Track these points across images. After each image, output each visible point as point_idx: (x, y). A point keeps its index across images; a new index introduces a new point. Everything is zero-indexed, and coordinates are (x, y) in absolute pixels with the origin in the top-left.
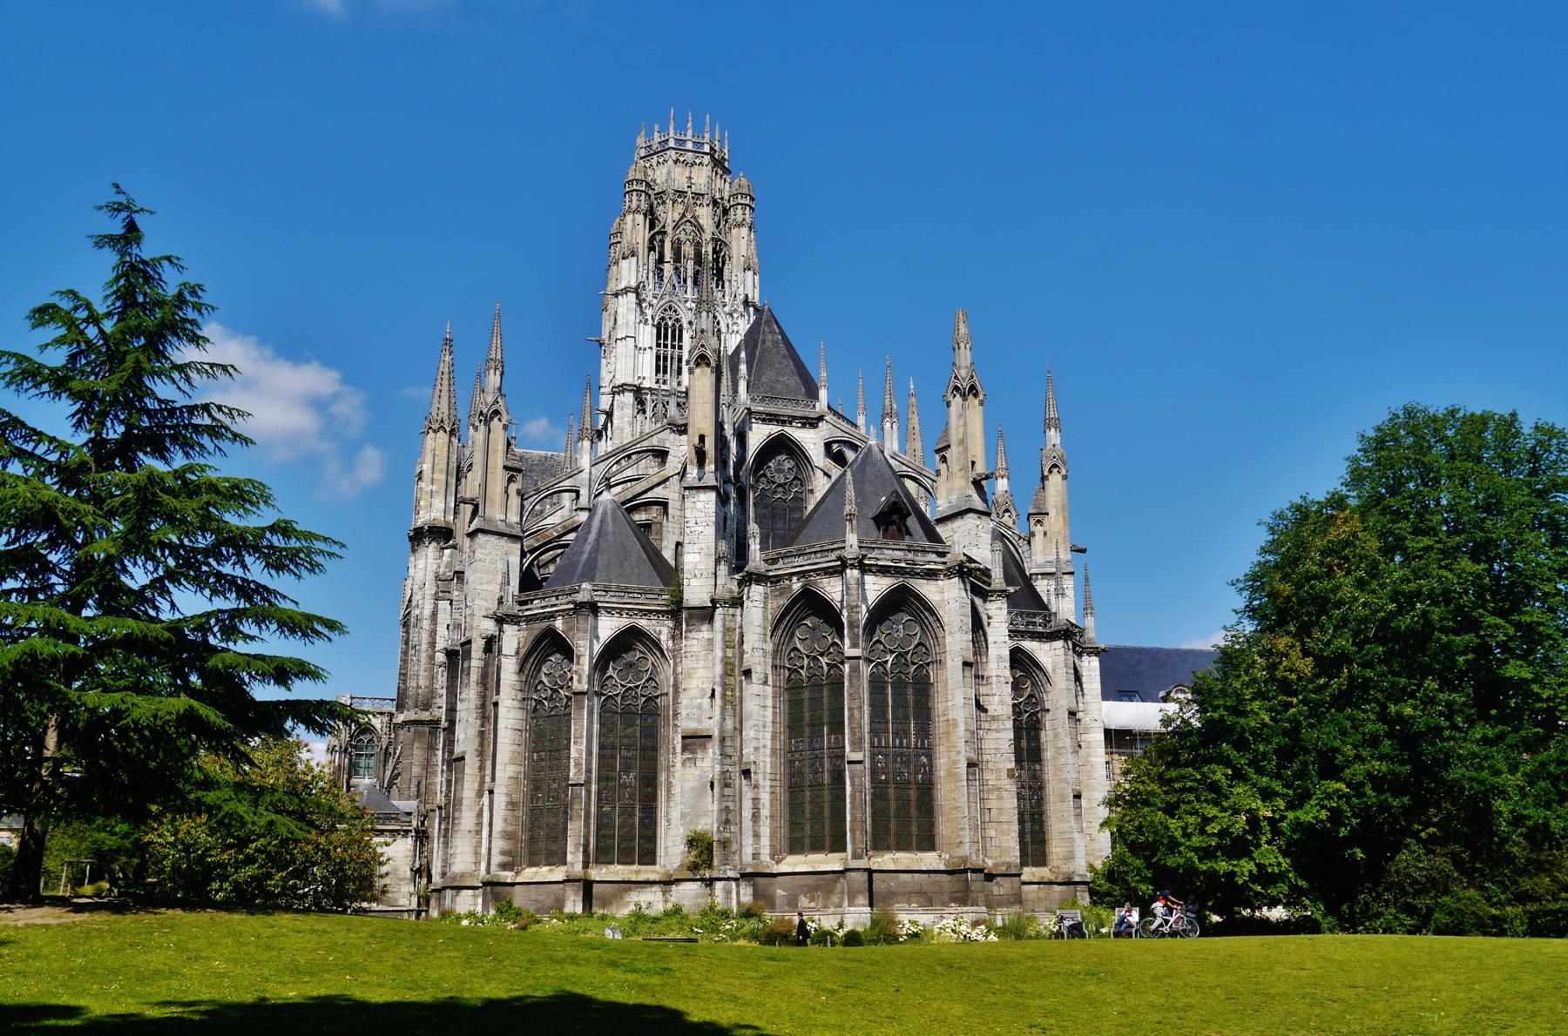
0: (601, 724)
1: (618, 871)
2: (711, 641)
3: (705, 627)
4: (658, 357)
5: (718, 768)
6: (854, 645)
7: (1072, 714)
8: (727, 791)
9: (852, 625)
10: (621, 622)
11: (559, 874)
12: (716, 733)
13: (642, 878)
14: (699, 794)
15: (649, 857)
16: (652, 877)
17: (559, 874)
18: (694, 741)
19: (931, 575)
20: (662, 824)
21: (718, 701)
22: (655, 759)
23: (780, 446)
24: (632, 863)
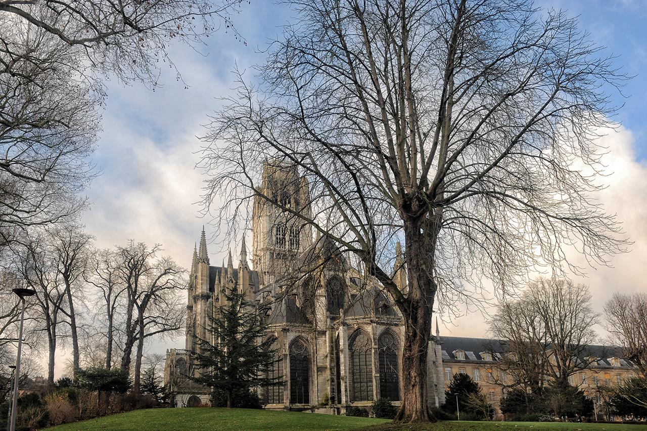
0: (291, 363)
1: (299, 405)
2: (326, 340)
3: (324, 336)
4: (277, 239)
5: (329, 377)
6: (375, 345)
7: (434, 362)
8: (333, 383)
9: (374, 339)
10: (297, 334)
11: (281, 406)
12: (328, 367)
13: (306, 407)
14: (324, 383)
15: (307, 401)
16: (309, 407)
17: (281, 406)
18: (321, 369)
19: (396, 325)
20: (310, 394)
21: (328, 359)
22: (307, 374)
23: (334, 278)
24: (302, 403)
